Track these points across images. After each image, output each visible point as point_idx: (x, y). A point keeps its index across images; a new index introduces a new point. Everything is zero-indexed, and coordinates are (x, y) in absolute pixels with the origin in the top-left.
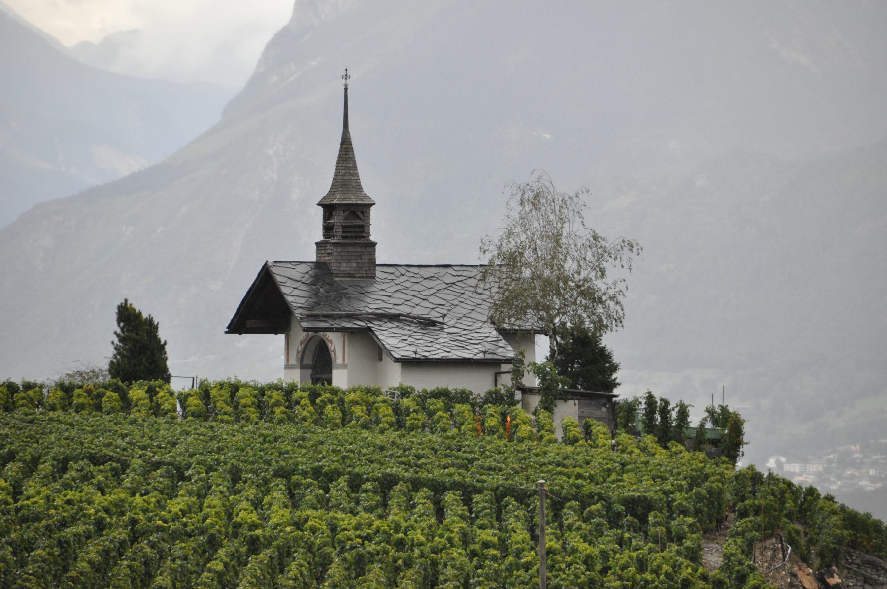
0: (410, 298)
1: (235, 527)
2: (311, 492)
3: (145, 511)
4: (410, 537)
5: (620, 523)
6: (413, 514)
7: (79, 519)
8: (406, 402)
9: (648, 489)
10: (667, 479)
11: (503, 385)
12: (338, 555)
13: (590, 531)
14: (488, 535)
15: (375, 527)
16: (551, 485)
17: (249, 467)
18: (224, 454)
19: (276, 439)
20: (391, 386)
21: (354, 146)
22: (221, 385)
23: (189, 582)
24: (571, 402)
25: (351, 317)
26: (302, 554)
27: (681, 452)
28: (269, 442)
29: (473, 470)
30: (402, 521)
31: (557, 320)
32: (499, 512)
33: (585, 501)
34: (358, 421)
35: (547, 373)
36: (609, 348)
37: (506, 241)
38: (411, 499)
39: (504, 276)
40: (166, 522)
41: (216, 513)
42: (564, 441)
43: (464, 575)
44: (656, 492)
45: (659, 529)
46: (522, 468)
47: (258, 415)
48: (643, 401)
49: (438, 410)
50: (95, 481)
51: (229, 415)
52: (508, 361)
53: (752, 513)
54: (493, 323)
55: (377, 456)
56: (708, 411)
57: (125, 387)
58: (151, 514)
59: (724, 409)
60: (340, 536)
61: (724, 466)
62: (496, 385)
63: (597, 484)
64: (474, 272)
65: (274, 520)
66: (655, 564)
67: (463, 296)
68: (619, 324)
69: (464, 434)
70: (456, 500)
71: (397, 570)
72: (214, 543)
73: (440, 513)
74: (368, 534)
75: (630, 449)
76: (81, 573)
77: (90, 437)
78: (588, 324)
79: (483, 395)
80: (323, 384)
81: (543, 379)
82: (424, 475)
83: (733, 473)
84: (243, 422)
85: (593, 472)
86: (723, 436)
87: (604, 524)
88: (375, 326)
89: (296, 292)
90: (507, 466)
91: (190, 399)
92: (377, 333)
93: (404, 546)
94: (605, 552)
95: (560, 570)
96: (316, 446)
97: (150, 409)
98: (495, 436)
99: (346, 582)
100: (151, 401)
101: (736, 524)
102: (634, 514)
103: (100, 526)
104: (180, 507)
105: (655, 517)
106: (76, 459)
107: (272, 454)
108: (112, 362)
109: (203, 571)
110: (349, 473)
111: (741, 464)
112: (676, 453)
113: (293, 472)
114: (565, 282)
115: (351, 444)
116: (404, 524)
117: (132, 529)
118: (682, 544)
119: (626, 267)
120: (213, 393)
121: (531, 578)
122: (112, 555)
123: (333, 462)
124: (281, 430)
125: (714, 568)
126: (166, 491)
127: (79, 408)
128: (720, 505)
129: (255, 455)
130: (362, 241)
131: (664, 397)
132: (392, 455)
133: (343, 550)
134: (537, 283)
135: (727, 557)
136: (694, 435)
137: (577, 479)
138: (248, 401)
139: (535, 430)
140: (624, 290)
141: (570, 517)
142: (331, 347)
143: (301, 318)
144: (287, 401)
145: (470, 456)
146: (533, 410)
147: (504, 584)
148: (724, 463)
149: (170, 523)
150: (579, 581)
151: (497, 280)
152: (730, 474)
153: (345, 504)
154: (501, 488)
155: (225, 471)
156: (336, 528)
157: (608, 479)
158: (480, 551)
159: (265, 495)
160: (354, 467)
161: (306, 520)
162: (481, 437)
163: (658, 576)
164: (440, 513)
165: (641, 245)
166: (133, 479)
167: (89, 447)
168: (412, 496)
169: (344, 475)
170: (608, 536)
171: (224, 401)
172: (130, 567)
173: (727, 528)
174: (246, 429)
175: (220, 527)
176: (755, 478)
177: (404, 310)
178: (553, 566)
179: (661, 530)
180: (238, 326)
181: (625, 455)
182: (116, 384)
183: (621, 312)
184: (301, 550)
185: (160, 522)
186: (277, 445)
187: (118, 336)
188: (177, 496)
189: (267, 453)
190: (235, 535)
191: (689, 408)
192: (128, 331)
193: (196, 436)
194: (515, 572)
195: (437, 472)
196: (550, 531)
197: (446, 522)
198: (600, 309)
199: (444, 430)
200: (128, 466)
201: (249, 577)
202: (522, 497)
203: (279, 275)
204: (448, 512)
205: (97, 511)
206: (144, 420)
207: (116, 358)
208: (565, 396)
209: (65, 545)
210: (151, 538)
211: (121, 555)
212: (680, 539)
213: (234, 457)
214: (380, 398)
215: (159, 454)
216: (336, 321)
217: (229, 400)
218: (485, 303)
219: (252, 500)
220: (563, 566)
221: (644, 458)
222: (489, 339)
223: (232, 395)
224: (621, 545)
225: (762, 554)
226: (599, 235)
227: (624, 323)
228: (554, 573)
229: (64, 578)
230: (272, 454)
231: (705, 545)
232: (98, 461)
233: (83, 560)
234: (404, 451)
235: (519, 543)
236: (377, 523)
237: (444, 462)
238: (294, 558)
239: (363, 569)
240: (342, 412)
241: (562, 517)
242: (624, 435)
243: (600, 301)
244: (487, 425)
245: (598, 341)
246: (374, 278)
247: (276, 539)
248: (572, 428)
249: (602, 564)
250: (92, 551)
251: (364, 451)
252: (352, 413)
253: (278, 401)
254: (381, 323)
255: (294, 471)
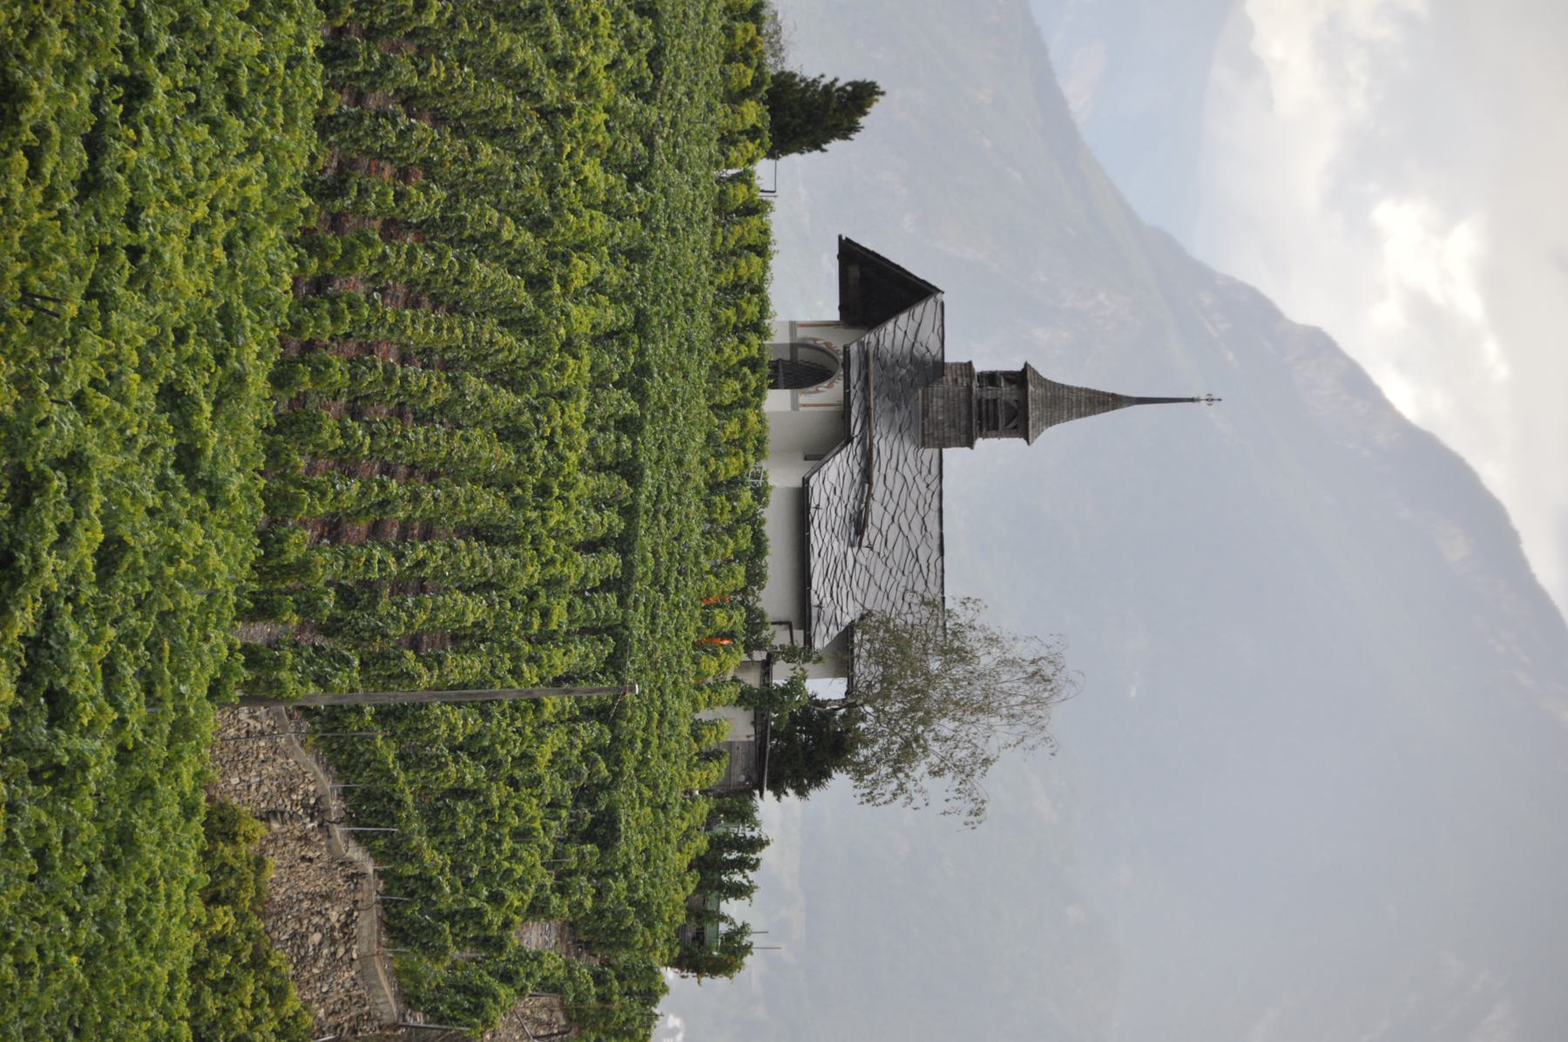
0: (895, 497)
1: (563, 255)
2: (616, 362)
3: (584, 128)
4: (555, 504)
5: (581, 804)
6: (587, 508)
7: (571, 35)
8: (747, 495)
9: (630, 843)
10: (646, 869)
11: (773, 634)
12: (527, 403)
13: (569, 761)
14: (559, 616)
15: (568, 454)
16: (633, 704)
17: (649, 274)
18: (667, 238)
19: (689, 311)
20: (769, 473)
21: (1111, 412)
22: (765, 232)
23: (485, 192)
24: (751, 731)
25: (866, 414)
26: (527, 352)
27: (684, 889)
28: (686, 302)
29: (652, 592)
30: (578, 492)
31: (868, 709)
32: (595, 631)
33: (611, 753)
34: (718, 427)
35: (792, 697)
36: (830, 783)
37: (981, 635)
38: (609, 506)
39: (930, 632)
40: (569, 157)
41: (583, 228)
42: (696, 722)
43: (501, 583)
44: (627, 854)
45: (574, 859)
46: (656, 662)
47: (724, 284)
48: (755, 834)
49: (736, 542)
50: (625, 55)
51: (723, 244)
52: (808, 640)
53: (600, 991)
54: (862, 617)
55: (669, 455)
56: (744, 926)
57: (760, 95)
58: (580, 136)
59: (747, 949)
60: (553, 404)
61: (666, 951)
62: (773, 623)
63: (636, 770)
64: (934, 589)
65: (575, 311)
66: (525, 854)
67: (900, 574)
68: (864, 799)
69: (702, 579)
70: (608, 570)
71: (508, 488)
72: (540, 225)
73: (590, 547)
74: (557, 445)
75: (687, 816)
76: (494, 40)
77: (688, 47)
78: (864, 752)
79: (759, 605)
80: (770, 377)
81: (783, 691)
82: (643, 522)
83: (656, 964)
84: (714, 263)
85: (652, 763)
86: (710, 949)
87: (579, 781)
88: (854, 449)
89: (900, 335)
90: (658, 641)
91: (744, 188)
92: (843, 452)
93: (542, 497)
94: (540, 782)
95: (513, 720)
96: (682, 368)
97: (729, 131)
98: (700, 624)
99: (489, 415)
100: (741, 133)
101: (584, 969)
102: (594, 823)
103: (561, 65)
104: (591, 177)
105: (591, 854)
106: (656, 28)
107: (669, 305)
108: (794, 76)
109: (500, 211)
110: (643, 416)
111: (670, 975)
112: (682, 882)
113: (643, 336)
114: (922, 721)
115: (685, 418)
116: (572, 495)
117: (558, 109)
118: (553, 892)
119: (947, 807)
120: (754, 221)
121: (499, 678)
122: (521, 82)
123: (659, 393)
124: (703, 318)
125: (521, 939)
126: (613, 157)
127: (729, 32)
128: (611, 946)
129: (666, 281)
130: (975, 428)
131: (762, 863)
132: (671, 476)
133: (534, 409)
134: (920, 682)
135: (537, 957)
136: (709, 908)
137: (642, 741)
138: (743, 271)
139: (710, 680)
140: (914, 804)
141: (589, 732)
142: (823, 387)
143: (862, 343)
144: (745, 326)
145: (671, 589)
146: (740, 678)
147: (492, 640)
148: (671, 950)
149: (567, 164)
150: (498, 747)
151: (924, 621)
152: (655, 959)
153: (599, 410)
154: (627, 633)
155: (643, 239)
156: (565, 399)
157: (643, 786)
158: (536, 604)
159: (610, 299)
160: (652, 422)
161: (575, 357)
162: (698, 603)
163: (507, 859)
164: (590, 547)
165: (979, 827)
166: (628, 110)
167: (673, 46)
168: (611, 506)
169: (641, 408)
170: (563, 786)
171: (743, 235)
172: (504, 107)
173: (578, 956)
174: (703, 268)
175: (563, 235)
176: (650, 995)
177: (878, 490)
178: (517, 709)
179: (572, 861)
180: (851, 255)
181: (677, 809)
182: (764, 82)
183: (881, 800)
184: (533, 351)
185: (568, 149)
186: (682, 313)
187: (833, 83)
188: (606, 171)
189: (669, 298)
190: (552, 256)
191: (747, 900)
192: (840, 97)
193: (691, 198)
194: (508, 655)
195: (647, 541)
196: (568, 704)
197: (577, 555)
198: (885, 770)
199: (707, 551)
200: (647, 102)
201: (492, 277)
202: (614, 663)
203: (925, 311)
204: (591, 559)
205: (582, 60)
206: (713, 123)
207: (801, 81)
208: (759, 722)
209: (533, 15)
210: (545, 137)
211: (521, 95)
212: (562, 889)
213: (663, 252)
214: (751, 459)
215: (666, 146)
216: (859, 394)
217: (745, 243)
218: (890, 604)
219: (602, 279)
220: (518, 724)
221: (674, 837)
222: (838, 612)
223: (750, 248)
224: (549, 805)
225: (544, 1006)
226: (990, 767)
227: (866, 804)
228: (508, 711)
229: (487, 14)
230: (669, 305)
231: (553, 924)
232: (654, 60)
233: (513, 41)
234: (676, 494)
235: (549, 661)
236: (573, 458)
237: (663, 551)
238: (521, 340)
239: (507, 439)
240: (731, 405)
241: (587, 721)
242: (707, 807)
243: (896, 771)
244: (716, 611)
245: (839, 767)
246: (924, 445)
247: (548, 314)
248: (714, 733)
249: (523, 779)
250: (526, 54)
251: (675, 437)
252: (729, 419)
253: (744, 313)
254: (859, 458)
255: (645, 338)
